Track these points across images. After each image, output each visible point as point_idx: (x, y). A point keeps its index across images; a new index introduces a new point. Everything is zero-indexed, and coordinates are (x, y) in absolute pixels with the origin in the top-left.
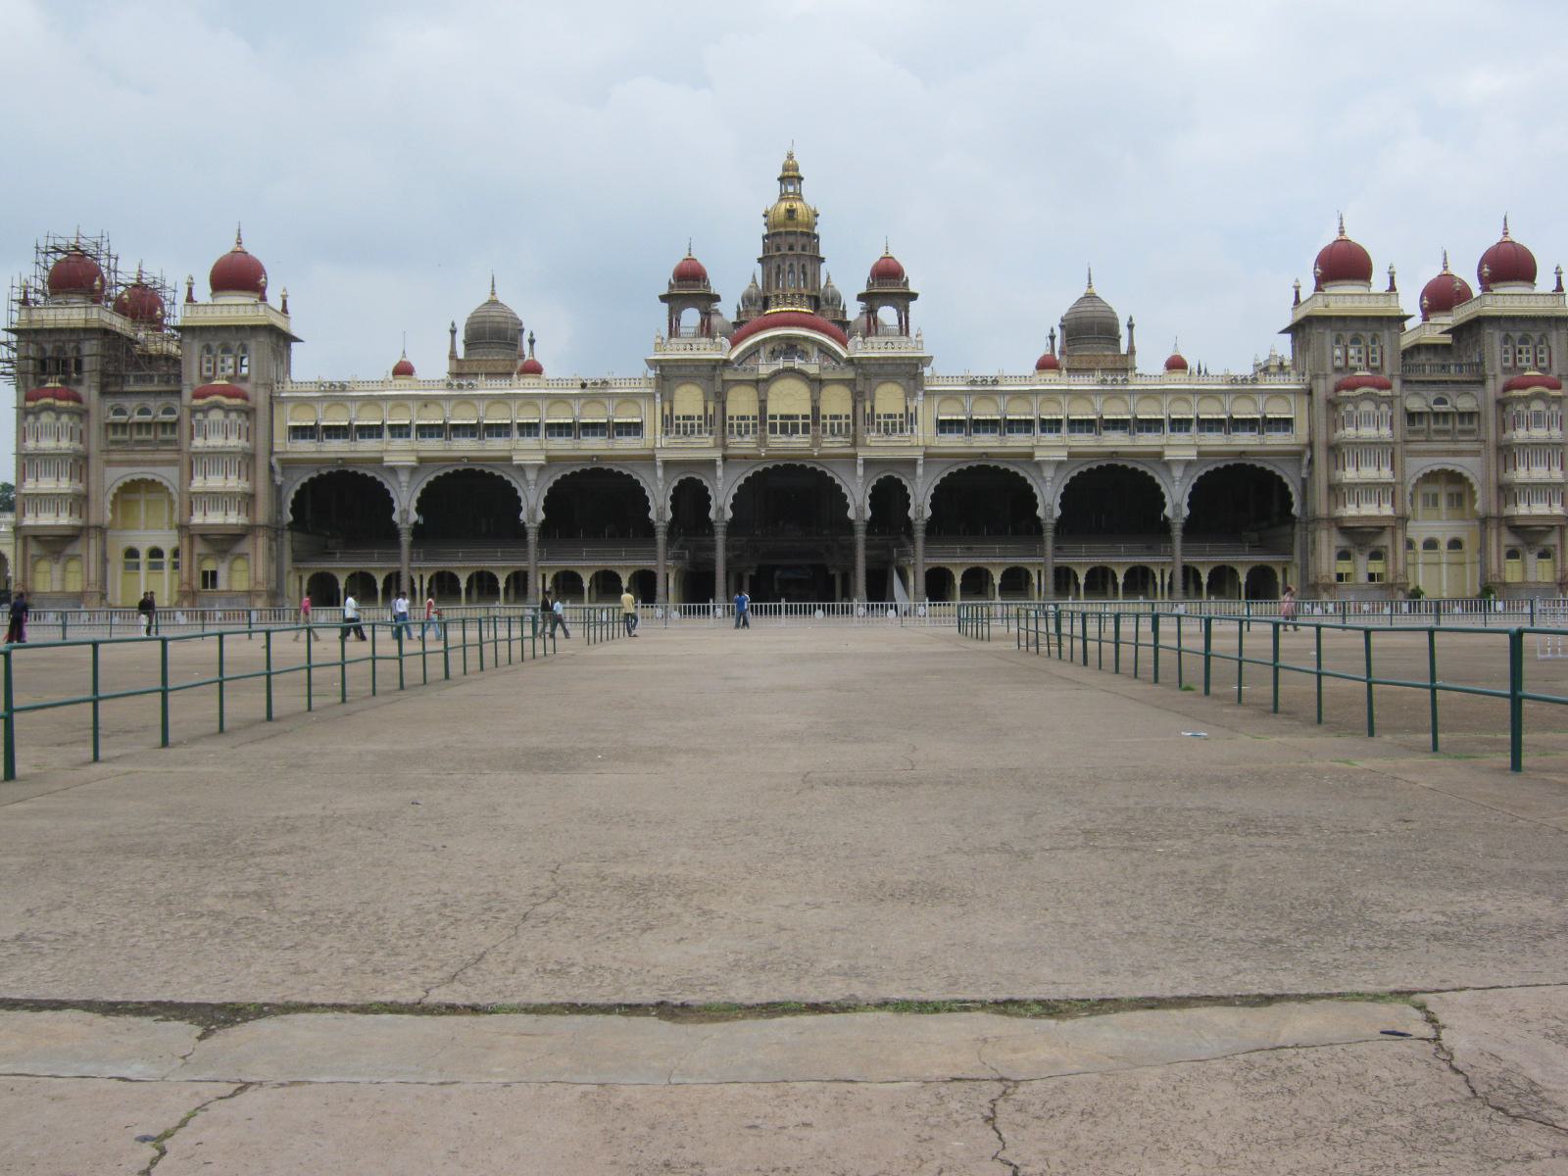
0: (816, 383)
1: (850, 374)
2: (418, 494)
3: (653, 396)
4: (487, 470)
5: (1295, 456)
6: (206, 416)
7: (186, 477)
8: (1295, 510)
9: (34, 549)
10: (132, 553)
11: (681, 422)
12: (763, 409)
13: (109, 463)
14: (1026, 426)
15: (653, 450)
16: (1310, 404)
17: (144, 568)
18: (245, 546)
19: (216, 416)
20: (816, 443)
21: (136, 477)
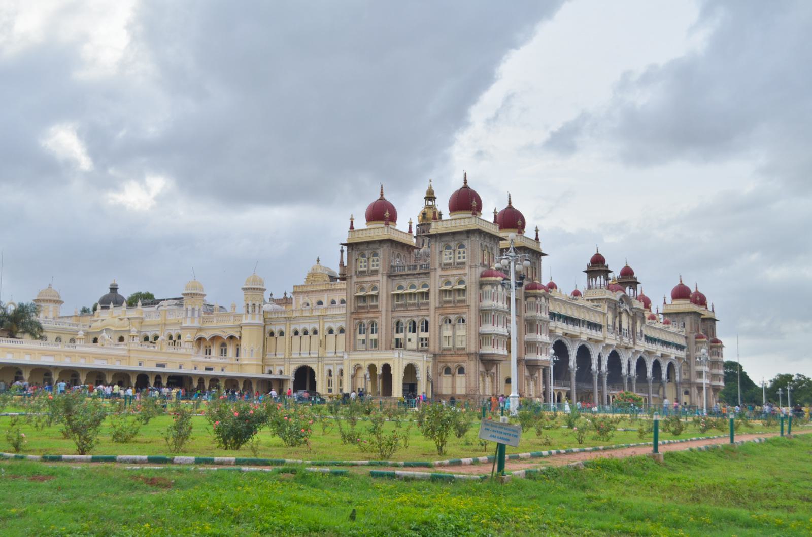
0: (628, 315)
1: (632, 315)
3: (604, 314)
8: (677, 378)
9: (482, 369)
15: (605, 338)
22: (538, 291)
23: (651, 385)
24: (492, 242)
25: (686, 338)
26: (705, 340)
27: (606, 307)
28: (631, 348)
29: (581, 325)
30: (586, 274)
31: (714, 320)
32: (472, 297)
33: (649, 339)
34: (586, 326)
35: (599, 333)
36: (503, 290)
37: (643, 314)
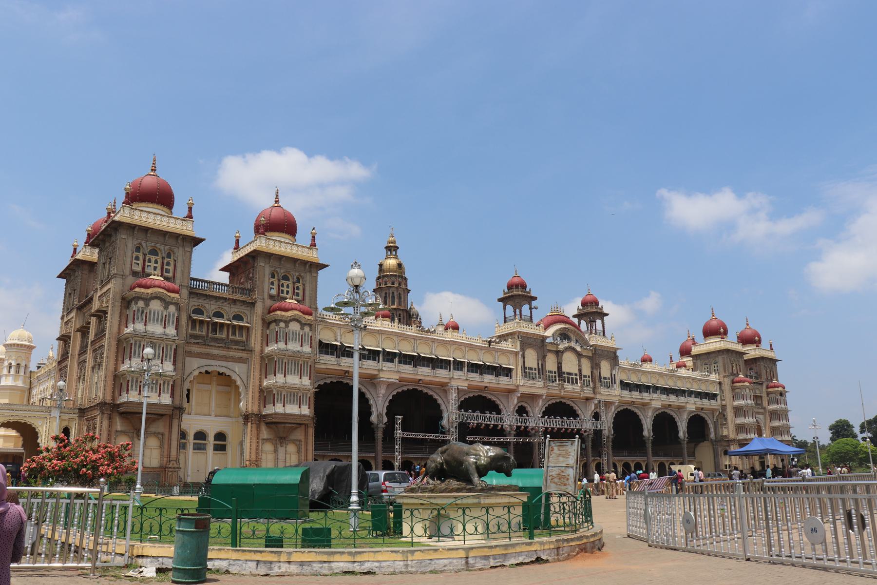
0: (579, 355)
1: (590, 355)
2: (387, 404)
3: (516, 353)
4: (425, 391)
5: (713, 411)
6: (287, 326)
7: (257, 374)
8: (712, 435)
10: (183, 435)
11: (527, 371)
12: (560, 368)
13: (191, 354)
14: (647, 388)
16: (720, 388)
17: (190, 447)
18: (299, 435)
19: (294, 327)
20: (582, 390)
21: (210, 369)
22: (278, 313)
23: (649, 446)
24: (172, 241)
25: (720, 383)
26: (747, 384)
27: (519, 343)
28: (592, 398)
29: (452, 367)
30: (502, 304)
31: (774, 361)
32: (112, 321)
33: (625, 385)
34: (465, 369)
35: (505, 378)
36: (166, 308)
37: (615, 353)
